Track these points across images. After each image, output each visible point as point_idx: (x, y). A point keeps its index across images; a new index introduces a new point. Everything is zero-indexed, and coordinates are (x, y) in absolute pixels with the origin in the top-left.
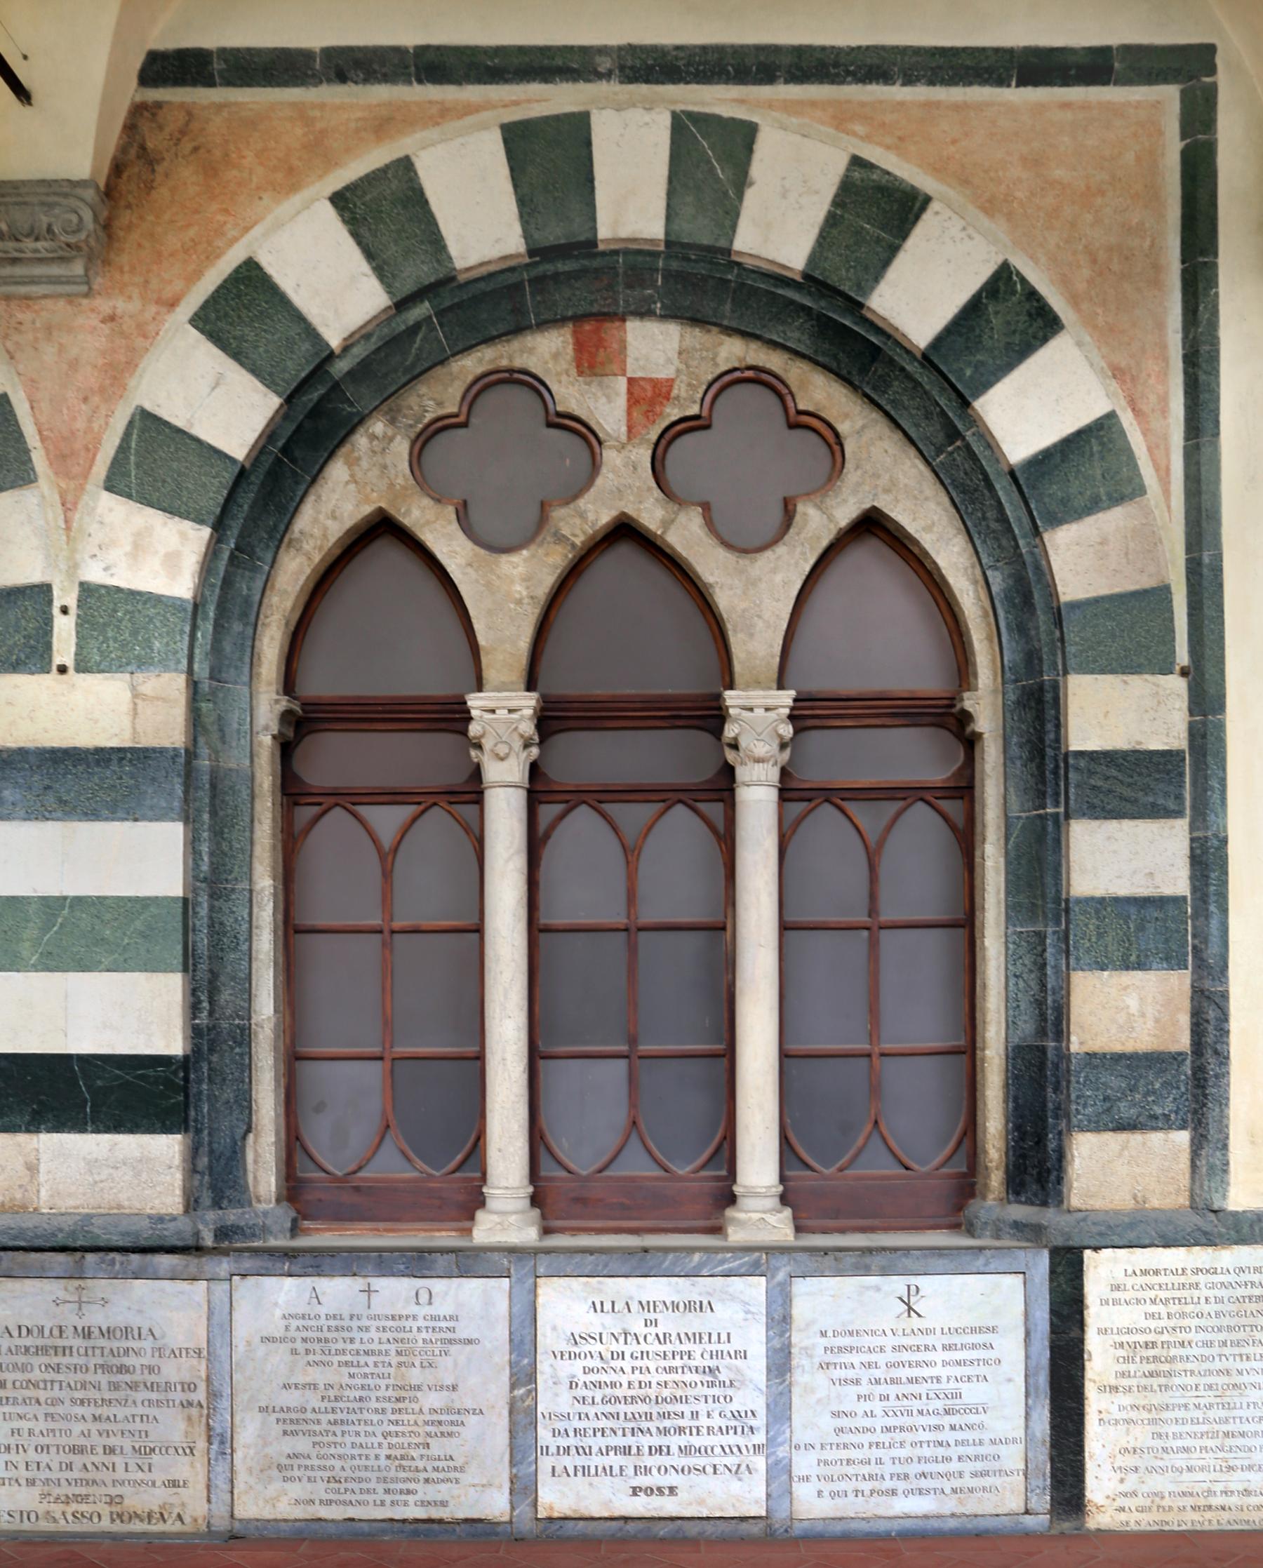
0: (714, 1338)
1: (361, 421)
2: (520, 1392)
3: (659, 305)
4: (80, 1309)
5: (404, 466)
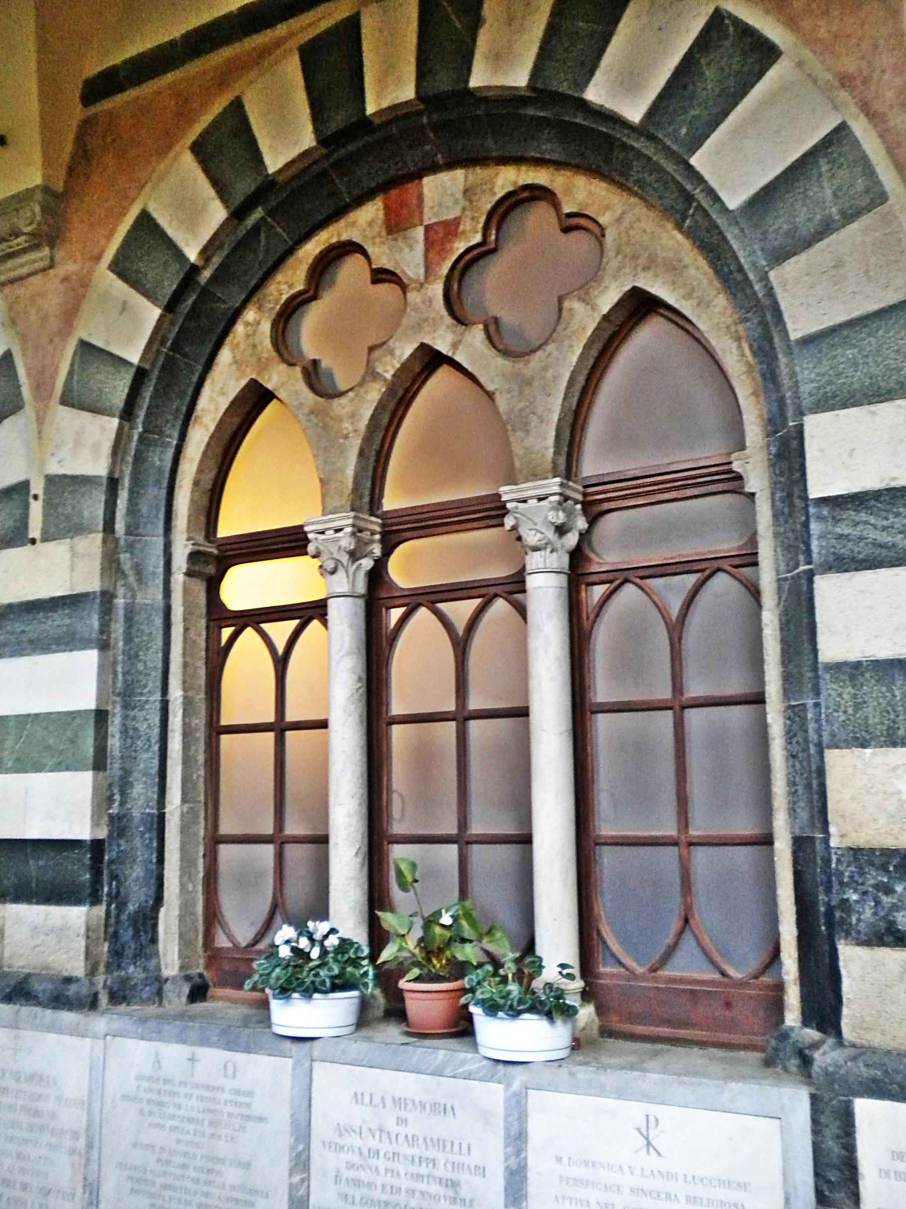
0: (456, 1147)
1: (236, 315)
2: (297, 1179)
3: (439, 156)
4: (15, 1055)
5: (267, 342)
